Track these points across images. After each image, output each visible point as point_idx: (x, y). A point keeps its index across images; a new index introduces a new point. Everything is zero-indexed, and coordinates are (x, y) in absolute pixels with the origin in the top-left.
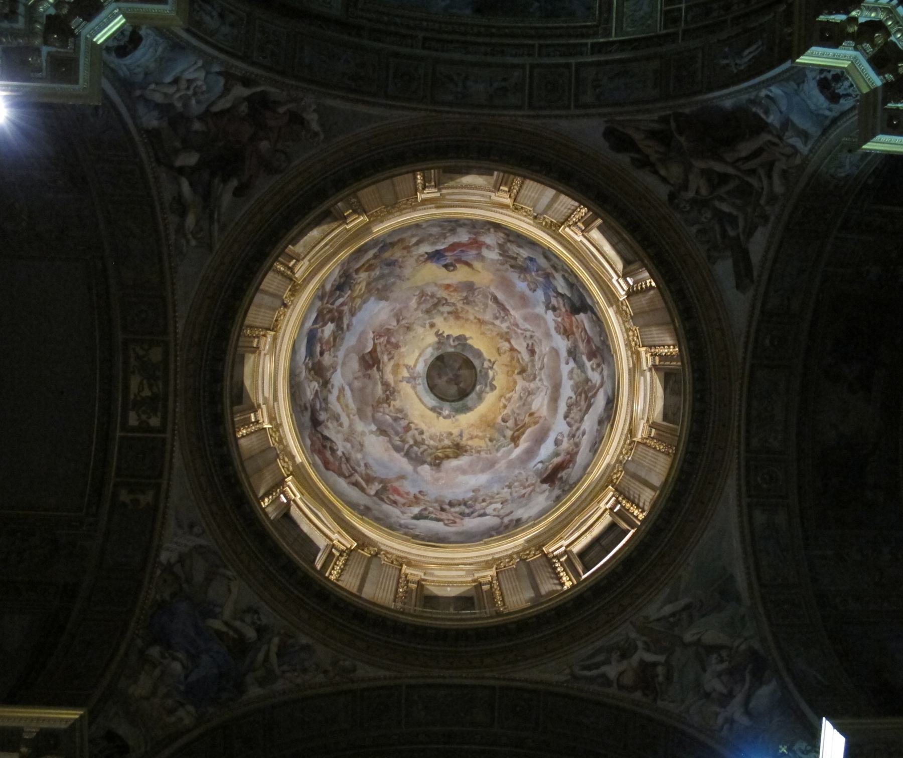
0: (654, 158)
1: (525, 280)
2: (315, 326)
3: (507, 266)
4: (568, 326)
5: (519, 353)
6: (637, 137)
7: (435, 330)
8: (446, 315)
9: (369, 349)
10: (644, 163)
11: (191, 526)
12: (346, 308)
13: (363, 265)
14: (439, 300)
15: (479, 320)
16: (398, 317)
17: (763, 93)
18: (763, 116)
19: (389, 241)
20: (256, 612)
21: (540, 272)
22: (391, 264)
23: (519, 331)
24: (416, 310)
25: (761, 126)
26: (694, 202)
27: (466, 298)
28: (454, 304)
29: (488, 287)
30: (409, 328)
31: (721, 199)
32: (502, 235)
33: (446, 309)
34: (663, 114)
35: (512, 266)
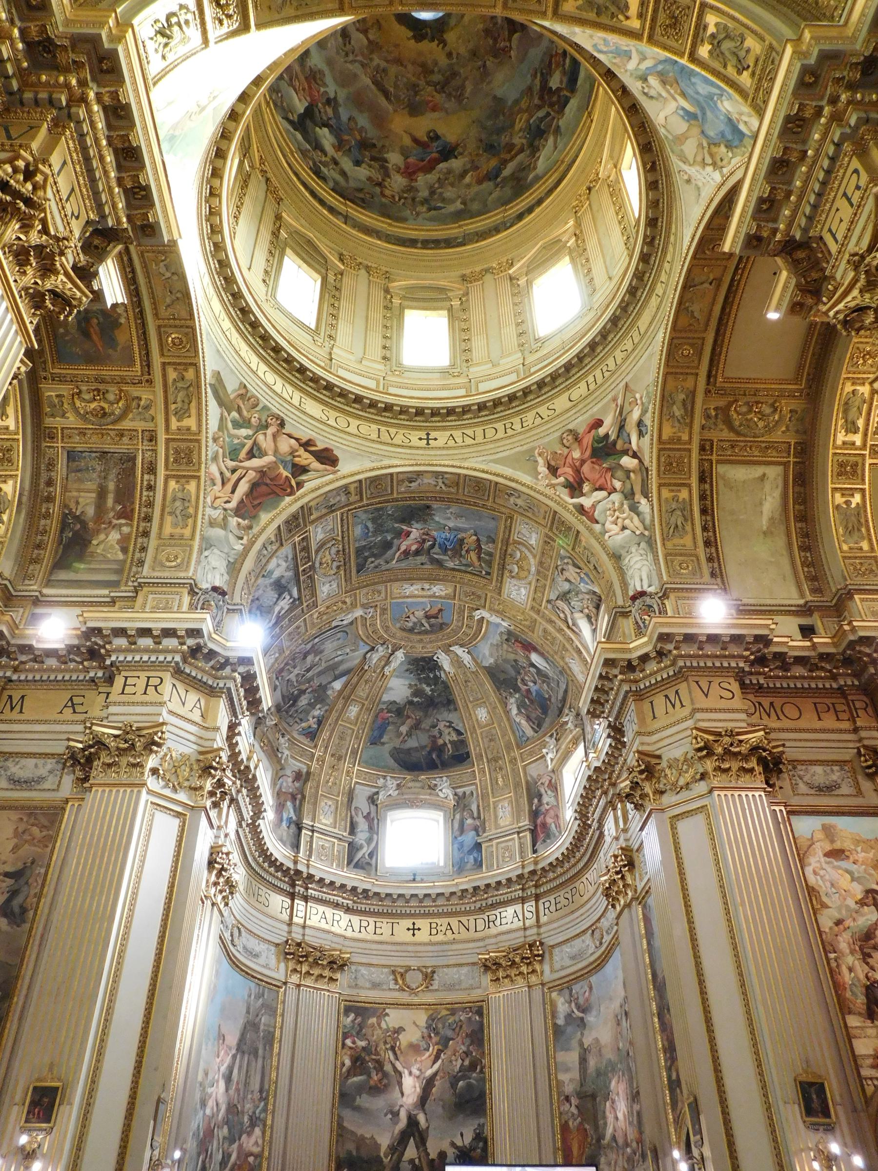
0: (301, 451)
1: (361, 130)
2: (568, 94)
3: (379, 145)
4: (314, 85)
5: (358, 30)
6: (316, 465)
7: (447, 49)
8: (436, 69)
9: (516, 35)
10: (307, 445)
11: (688, 181)
12: (536, 101)
13: (516, 155)
14: (442, 91)
15: (402, 65)
16: (485, 74)
17: (245, 541)
18: (240, 520)
19: (491, 184)
20: (645, 94)
21: (347, 147)
22: (491, 148)
23: (360, 58)
24: (466, 78)
25: (239, 512)
26: (267, 427)
27: (416, 93)
28: (428, 83)
29: (395, 111)
30: (474, 54)
31: (247, 437)
32: (387, 192)
33: (437, 77)
34: (301, 491)
35: (374, 146)
